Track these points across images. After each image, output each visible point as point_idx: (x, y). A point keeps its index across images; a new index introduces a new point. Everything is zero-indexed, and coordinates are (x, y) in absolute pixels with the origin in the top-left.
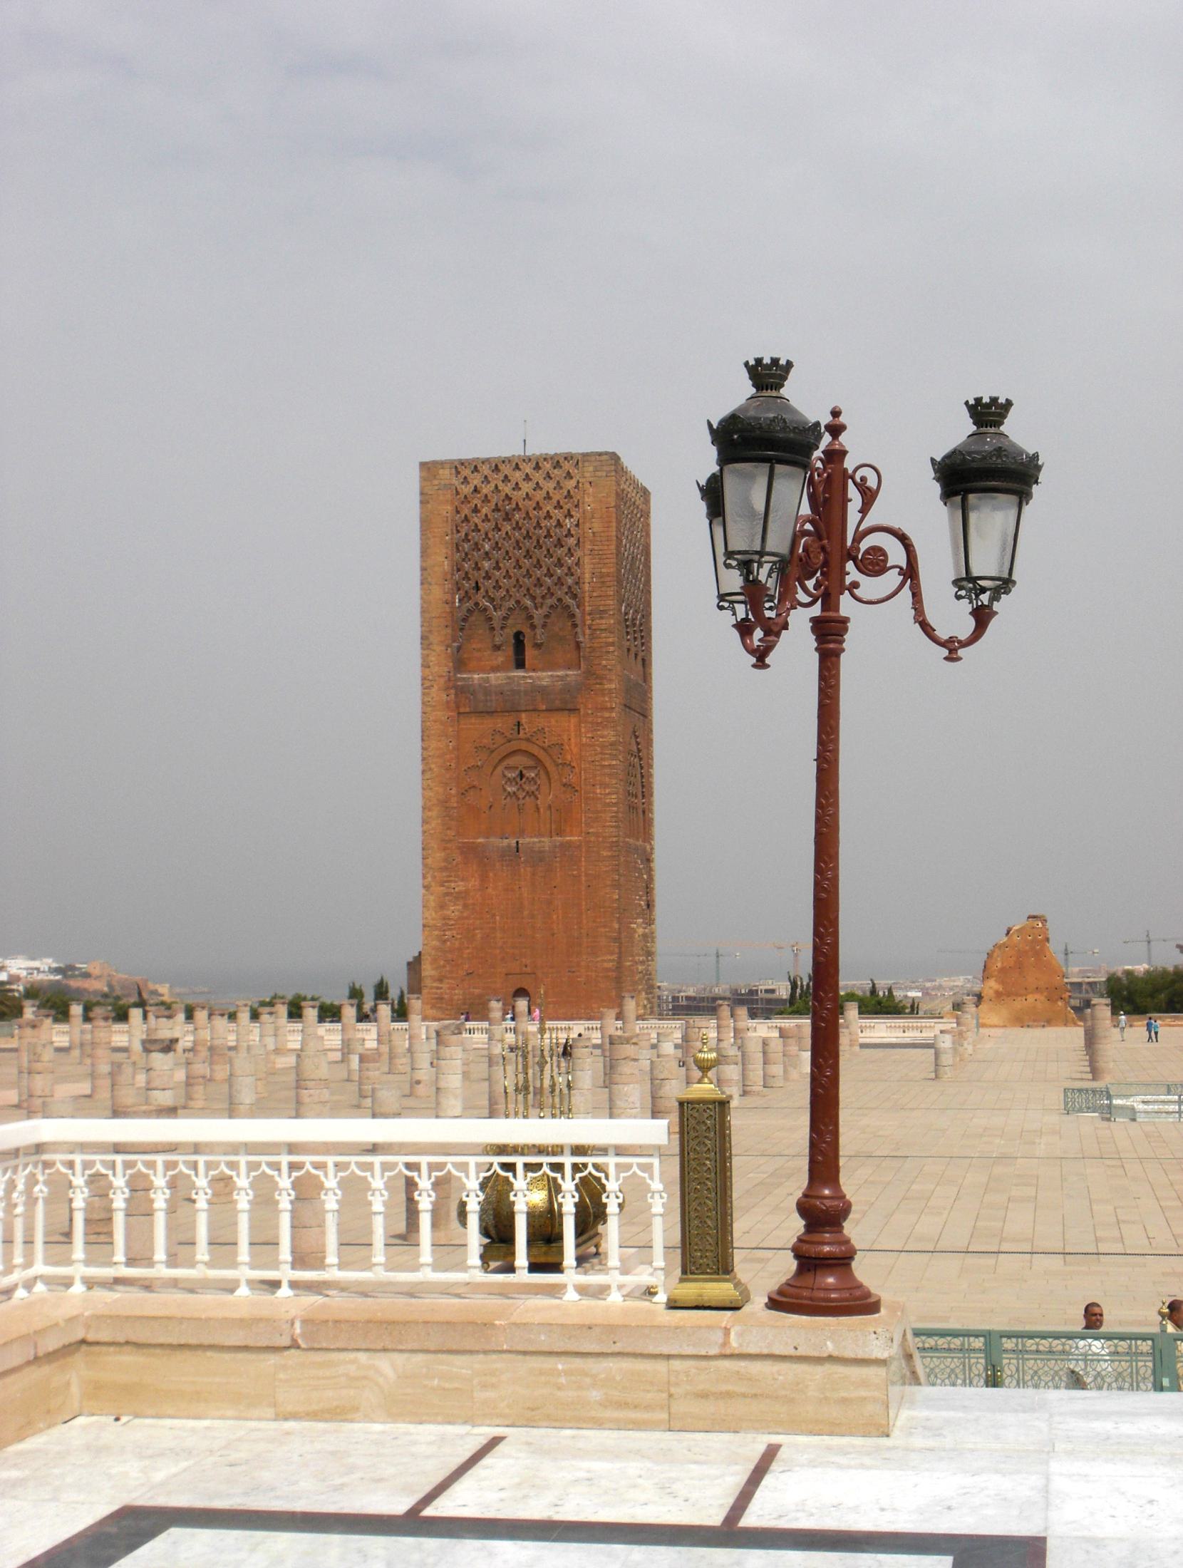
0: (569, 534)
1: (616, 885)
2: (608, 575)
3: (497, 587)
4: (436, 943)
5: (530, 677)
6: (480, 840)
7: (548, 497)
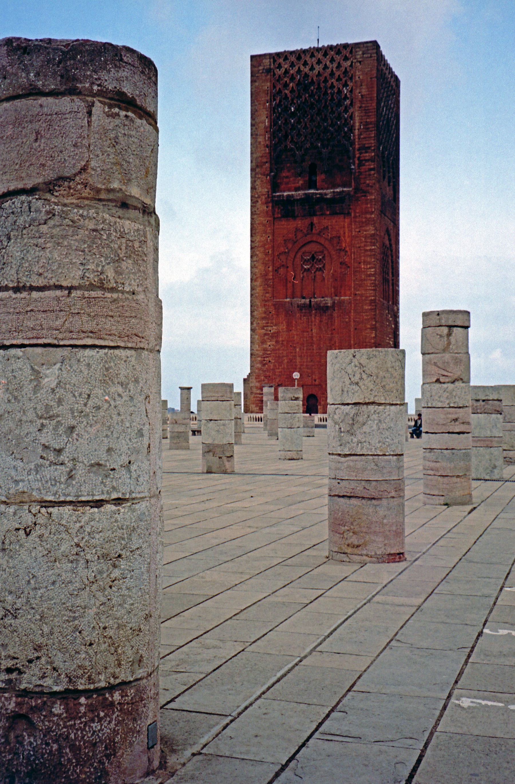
0: (346, 98)
1: (374, 328)
2: (371, 123)
3: (299, 135)
4: (259, 366)
5: (320, 194)
6: (288, 300)
7: (332, 74)
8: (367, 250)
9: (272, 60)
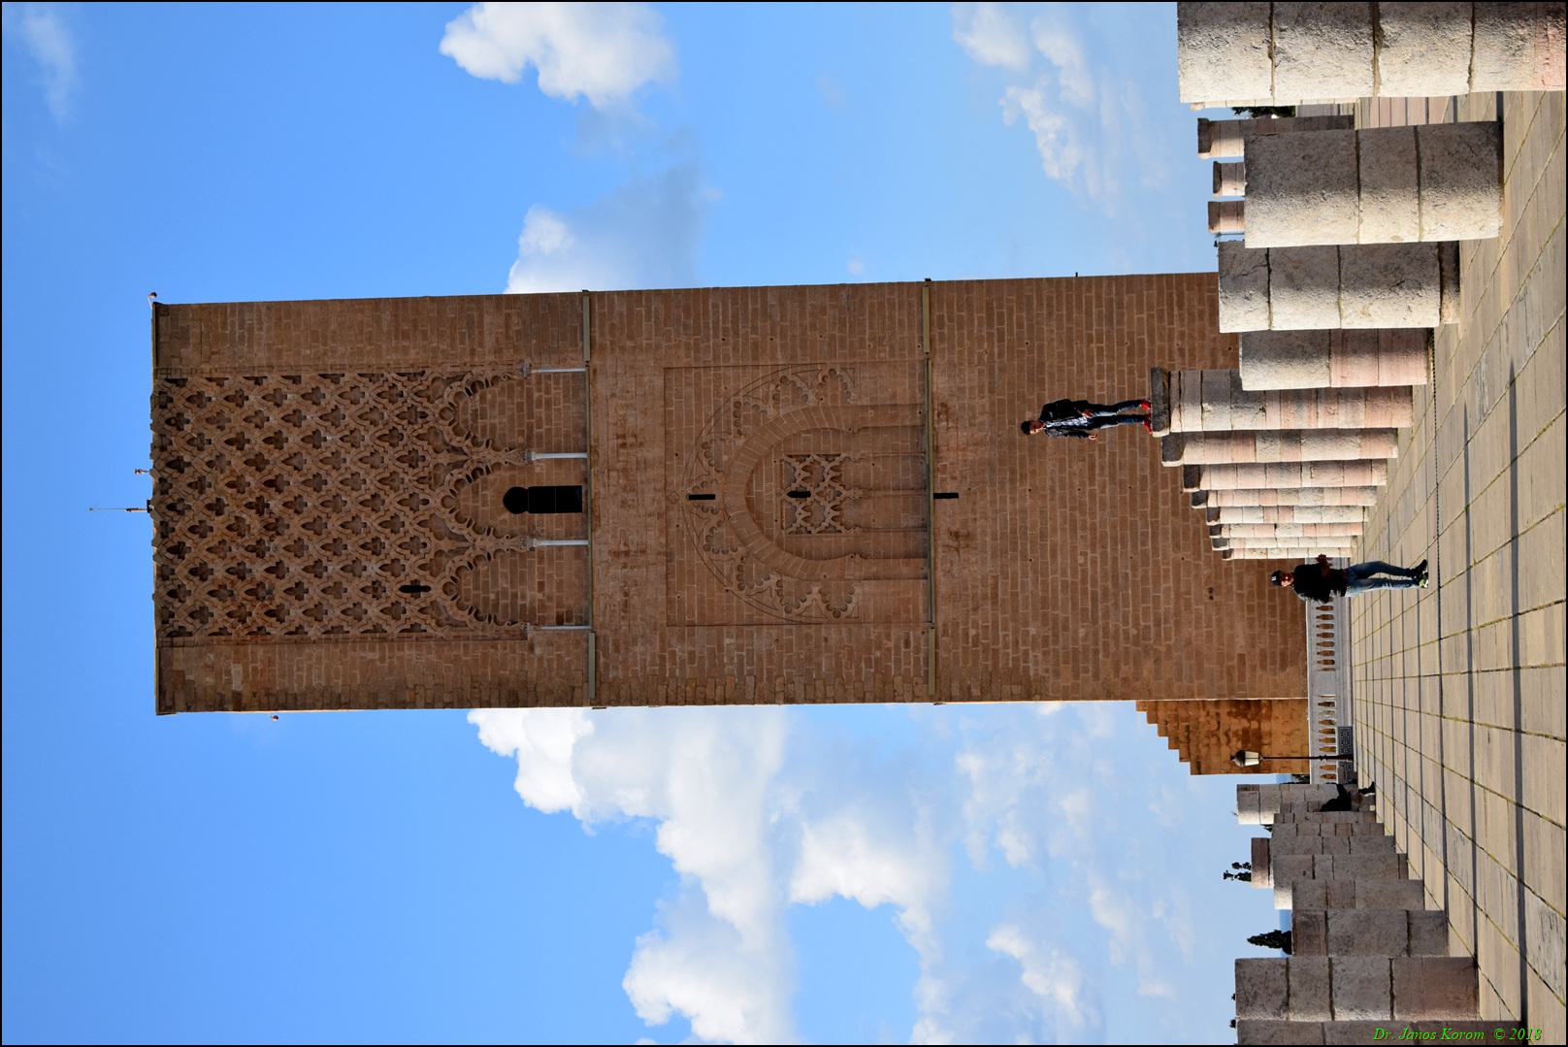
9: (178, 640)
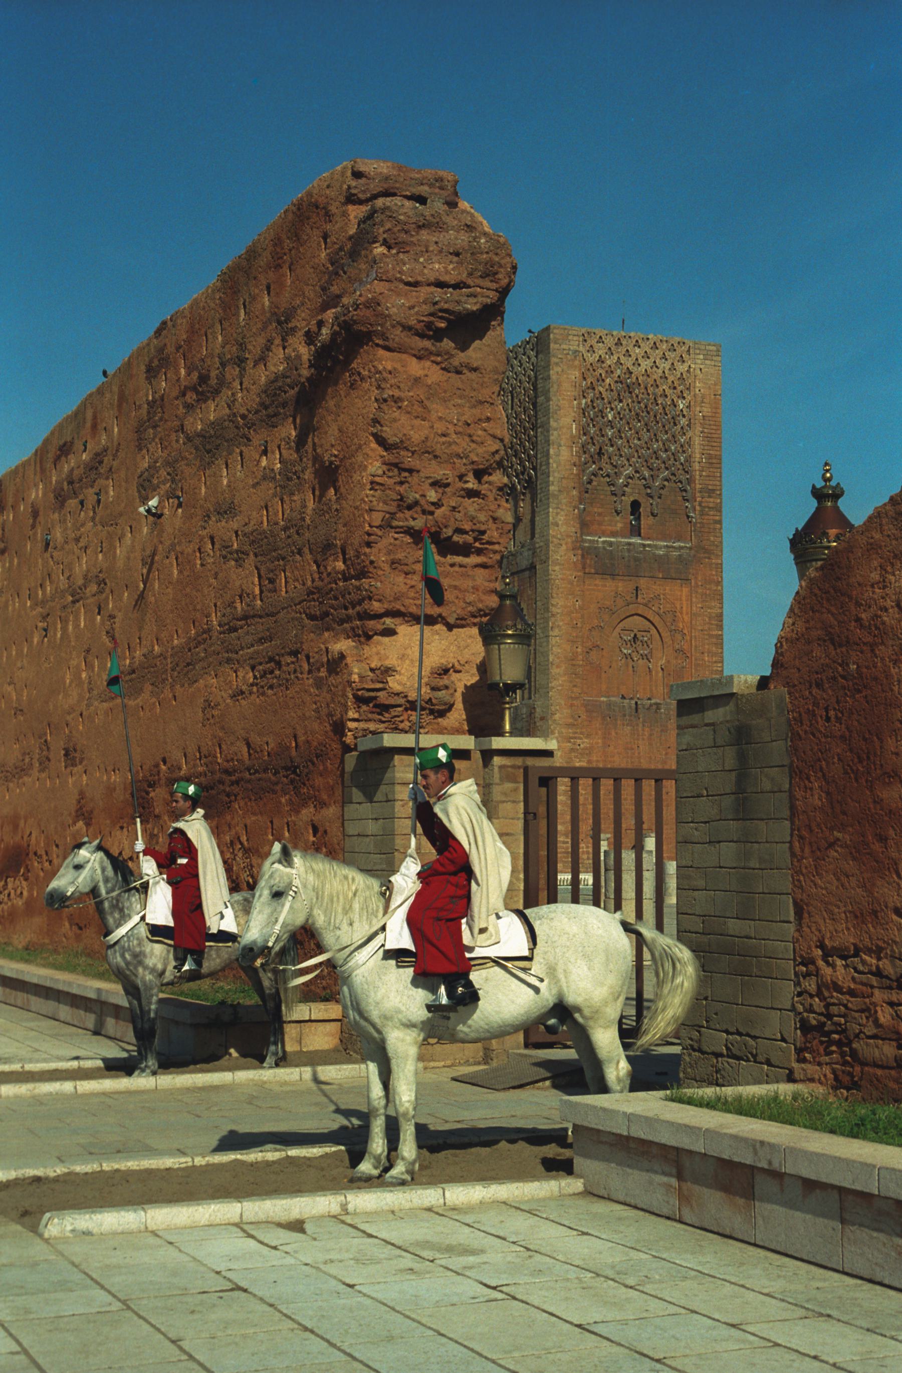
5: (649, 546)
8: (711, 636)
